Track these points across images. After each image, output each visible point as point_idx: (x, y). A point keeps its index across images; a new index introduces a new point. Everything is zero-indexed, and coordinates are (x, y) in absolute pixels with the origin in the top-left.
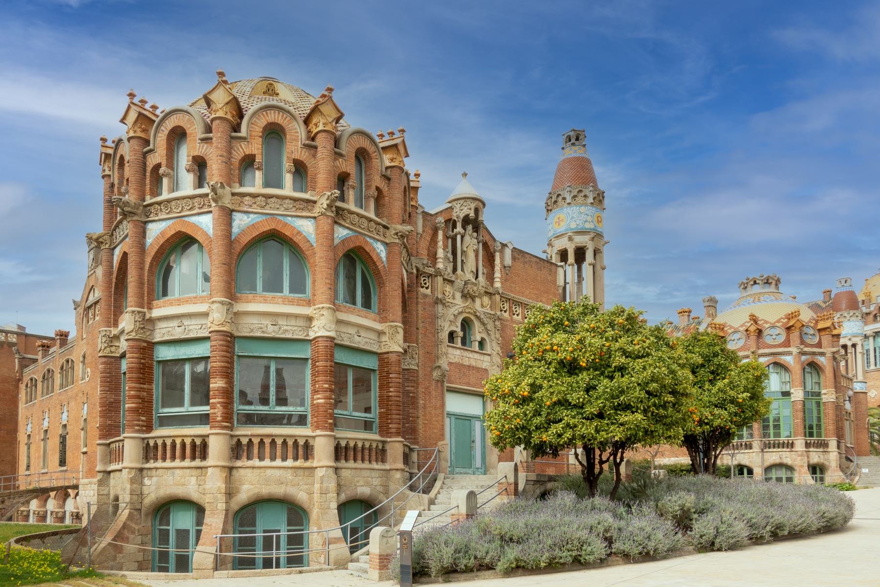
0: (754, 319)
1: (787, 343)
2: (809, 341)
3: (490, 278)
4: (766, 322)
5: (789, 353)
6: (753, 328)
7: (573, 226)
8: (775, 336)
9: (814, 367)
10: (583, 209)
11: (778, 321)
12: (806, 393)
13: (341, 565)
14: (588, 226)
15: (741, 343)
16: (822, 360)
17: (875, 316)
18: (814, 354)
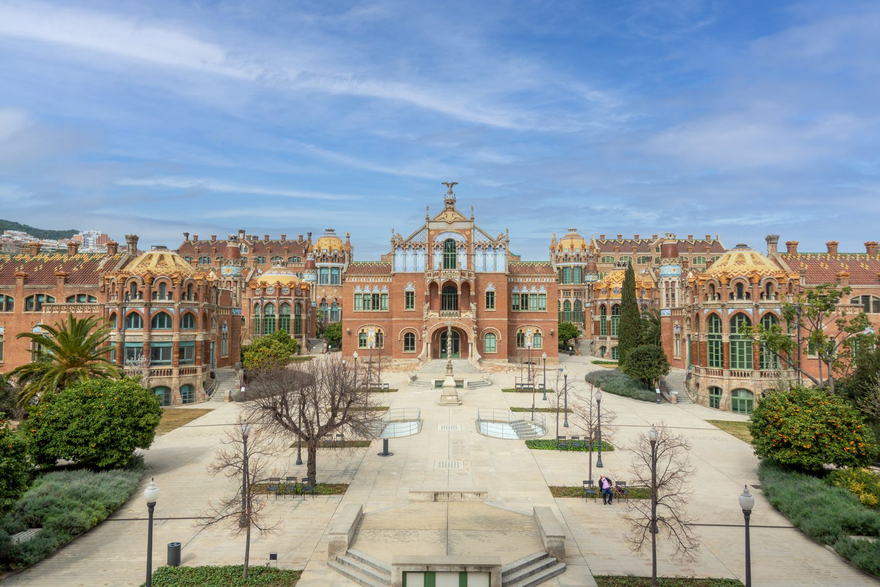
0: (278, 283)
1: (290, 295)
2: (298, 294)
3: (217, 303)
4: (283, 284)
5: (291, 299)
6: (278, 287)
7: (234, 273)
8: (286, 291)
9: (299, 304)
10: (237, 268)
11: (287, 285)
12: (296, 316)
13: (208, 400)
14: (239, 274)
15: (273, 292)
16: (303, 302)
17: (321, 259)
18: (299, 299)
